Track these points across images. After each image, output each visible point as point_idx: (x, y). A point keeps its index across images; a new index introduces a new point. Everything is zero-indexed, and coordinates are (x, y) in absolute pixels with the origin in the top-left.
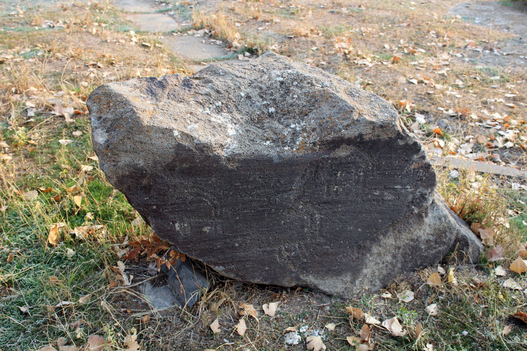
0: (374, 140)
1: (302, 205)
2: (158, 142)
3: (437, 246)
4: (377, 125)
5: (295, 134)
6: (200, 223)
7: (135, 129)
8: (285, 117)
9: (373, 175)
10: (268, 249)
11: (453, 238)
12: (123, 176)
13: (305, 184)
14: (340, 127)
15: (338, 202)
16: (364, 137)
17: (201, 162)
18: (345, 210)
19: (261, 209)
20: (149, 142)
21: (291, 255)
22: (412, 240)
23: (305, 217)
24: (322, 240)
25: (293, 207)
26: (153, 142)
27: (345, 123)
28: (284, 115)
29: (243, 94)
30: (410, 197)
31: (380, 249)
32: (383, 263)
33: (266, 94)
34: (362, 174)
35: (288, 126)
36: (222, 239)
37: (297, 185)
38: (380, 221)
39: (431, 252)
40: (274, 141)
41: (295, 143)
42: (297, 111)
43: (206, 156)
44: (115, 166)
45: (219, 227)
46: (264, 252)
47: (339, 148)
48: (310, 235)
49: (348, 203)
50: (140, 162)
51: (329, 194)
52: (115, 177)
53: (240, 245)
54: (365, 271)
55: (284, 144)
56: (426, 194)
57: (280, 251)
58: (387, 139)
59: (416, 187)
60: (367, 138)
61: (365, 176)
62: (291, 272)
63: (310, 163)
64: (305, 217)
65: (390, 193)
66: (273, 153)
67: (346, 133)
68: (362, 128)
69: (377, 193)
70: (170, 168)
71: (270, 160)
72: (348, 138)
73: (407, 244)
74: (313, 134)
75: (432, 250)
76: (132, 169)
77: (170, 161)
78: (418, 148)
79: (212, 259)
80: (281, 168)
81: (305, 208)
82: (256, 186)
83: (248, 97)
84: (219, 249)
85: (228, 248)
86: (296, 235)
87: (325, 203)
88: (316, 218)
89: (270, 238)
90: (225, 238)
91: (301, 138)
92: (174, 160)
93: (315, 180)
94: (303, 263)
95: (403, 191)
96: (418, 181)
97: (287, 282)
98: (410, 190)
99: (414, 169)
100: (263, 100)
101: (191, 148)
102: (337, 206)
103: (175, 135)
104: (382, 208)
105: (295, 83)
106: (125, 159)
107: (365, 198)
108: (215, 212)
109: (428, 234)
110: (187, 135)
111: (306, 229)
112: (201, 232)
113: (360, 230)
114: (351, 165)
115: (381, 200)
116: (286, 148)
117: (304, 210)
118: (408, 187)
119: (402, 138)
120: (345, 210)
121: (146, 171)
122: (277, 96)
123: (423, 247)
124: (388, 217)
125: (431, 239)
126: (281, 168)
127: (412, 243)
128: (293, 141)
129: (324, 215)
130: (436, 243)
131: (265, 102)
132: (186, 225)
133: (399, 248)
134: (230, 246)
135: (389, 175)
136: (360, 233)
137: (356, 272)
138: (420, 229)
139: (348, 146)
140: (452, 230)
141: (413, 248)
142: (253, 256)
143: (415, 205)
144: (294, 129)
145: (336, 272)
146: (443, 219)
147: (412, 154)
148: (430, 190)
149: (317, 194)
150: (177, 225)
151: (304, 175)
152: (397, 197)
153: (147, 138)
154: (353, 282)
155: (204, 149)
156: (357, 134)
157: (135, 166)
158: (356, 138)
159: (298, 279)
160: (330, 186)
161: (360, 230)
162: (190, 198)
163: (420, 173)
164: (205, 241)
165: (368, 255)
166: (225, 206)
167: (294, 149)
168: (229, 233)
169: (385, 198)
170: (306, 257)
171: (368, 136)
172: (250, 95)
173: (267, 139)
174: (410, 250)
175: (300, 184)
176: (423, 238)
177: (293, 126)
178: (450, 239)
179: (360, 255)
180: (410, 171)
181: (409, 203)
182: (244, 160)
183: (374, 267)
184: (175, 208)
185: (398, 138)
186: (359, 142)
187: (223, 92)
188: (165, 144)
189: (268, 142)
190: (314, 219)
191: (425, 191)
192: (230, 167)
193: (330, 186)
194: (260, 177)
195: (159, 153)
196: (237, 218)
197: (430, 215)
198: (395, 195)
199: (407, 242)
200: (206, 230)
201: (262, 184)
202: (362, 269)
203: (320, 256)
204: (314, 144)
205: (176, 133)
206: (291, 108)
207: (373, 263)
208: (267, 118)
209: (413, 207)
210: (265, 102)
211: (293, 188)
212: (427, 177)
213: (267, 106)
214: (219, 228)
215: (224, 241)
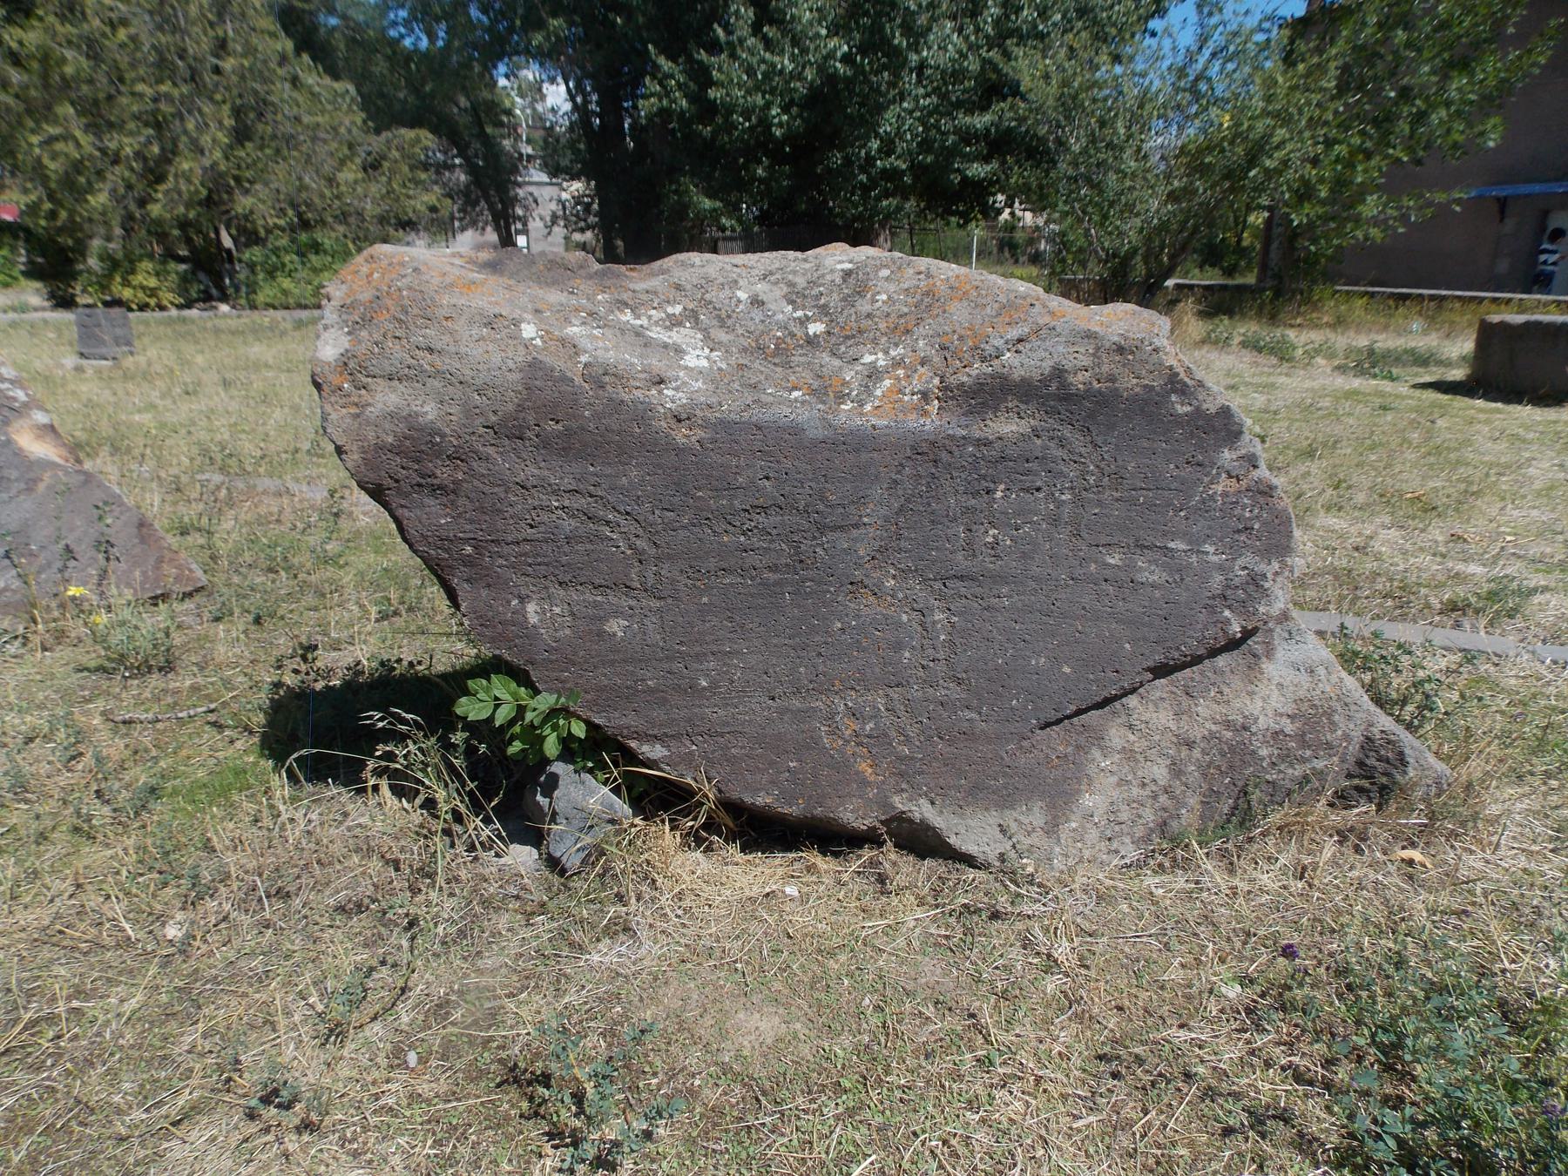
0: (1099, 391)
1: (894, 577)
2: (477, 351)
3: (1308, 753)
4: (1107, 345)
5: (874, 374)
6: (596, 605)
7: (416, 311)
8: (849, 343)
9: (1100, 503)
10: (796, 703)
11: (1357, 736)
12: (380, 447)
14: (999, 343)
16: (1071, 379)
17: (597, 416)
18: (1020, 605)
19: (772, 576)
20: (452, 349)
21: (863, 729)
22: (1228, 724)
23: (905, 618)
24: (955, 692)
25: (866, 581)
26: (463, 350)
27: (1014, 333)
28: (847, 338)
29: (742, 295)
30: (1217, 580)
31: (1132, 738)
32: (1144, 785)
33: (805, 297)
36: (660, 660)
39: (1290, 771)
40: (813, 392)
42: (882, 326)
43: (610, 399)
44: (358, 416)
45: (651, 623)
46: (782, 712)
47: (996, 409)
48: (921, 673)
49: (1030, 582)
50: (427, 408)
51: (970, 549)
52: (355, 448)
53: (714, 685)
54: (1088, 801)
55: (841, 398)
56: (1264, 576)
57: (831, 716)
58: (1137, 390)
59: (1235, 551)
60: (1078, 381)
61: (1078, 501)
62: (864, 783)
63: (913, 448)
64: (905, 618)
65: (1155, 562)
66: (803, 416)
67: (1016, 363)
68: (1061, 349)
69: (1114, 560)
70: (510, 431)
71: (796, 430)
72: (1023, 380)
74: (922, 370)
75: (1291, 765)
76: (402, 428)
77: (511, 407)
79: (631, 720)
80: (826, 454)
82: (756, 503)
83: (757, 302)
84: (652, 691)
85: (677, 688)
87: (962, 578)
88: (934, 623)
90: (669, 659)
91: (887, 383)
92: (521, 408)
94: (901, 759)
95: (1194, 558)
96: (1239, 531)
97: (852, 811)
98: (1215, 559)
99: (1225, 494)
100: (795, 310)
101: (569, 374)
102: (995, 592)
104: (1131, 606)
106: (386, 399)
107: (1078, 572)
108: (641, 575)
109: (1278, 714)
110: (563, 342)
111: (907, 654)
112: (600, 634)
113: (1067, 670)
115: (1128, 584)
117: (901, 595)
118: (1210, 548)
119: (1183, 391)
120: (1020, 605)
121: (443, 436)
122: (834, 300)
123: (1264, 752)
124: (1153, 636)
125: (1288, 730)
126: (826, 454)
127: (1229, 734)
128: (868, 390)
129: (960, 614)
130: (1304, 744)
131: (799, 314)
132: (557, 610)
133: (1190, 745)
134: (684, 683)
135: (1151, 506)
137: (1059, 797)
138: (1251, 694)
139: (1023, 407)
140: (1353, 707)
141: (1232, 749)
142: (750, 721)
143: (1229, 607)
145: (991, 789)
147: (1218, 448)
148: (1276, 566)
150: (531, 608)
152: (1177, 577)
153: (447, 338)
154: (1052, 829)
155: (607, 379)
156: (1047, 366)
157: (410, 418)
158: (1045, 381)
159: (886, 805)
160: (974, 527)
161: (1067, 670)
162: (569, 524)
163: (1243, 509)
164: (612, 663)
165: (1096, 753)
166: (669, 557)
167: (868, 407)
168: (681, 643)
169: (1142, 577)
170: (908, 740)
173: (795, 388)
174: (1223, 755)
175: (884, 511)
177: (868, 359)
178: (1346, 737)
179: (1070, 749)
180: (1212, 498)
181: (1214, 597)
182: (721, 421)
183: (1115, 794)
184: (525, 554)
185: (1174, 391)
186: (1052, 395)
187: (689, 287)
188: (496, 359)
189: (796, 394)
191: (1262, 567)
192: (680, 440)
193: (974, 527)
194: (767, 478)
195: (478, 382)
196: (705, 600)
197: (1280, 654)
199: (1214, 728)
200: (616, 628)
201: (774, 498)
202: (1078, 792)
203: (951, 742)
204: (925, 396)
205: (528, 331)
206: (866, 323)
207: (1114, 779)
208: (802, 346)
209: (1227, 613)
210: (799, 314)
212: (1264, 524)
213: (804, 322)
214: (651, 626)
215: (666, 666)
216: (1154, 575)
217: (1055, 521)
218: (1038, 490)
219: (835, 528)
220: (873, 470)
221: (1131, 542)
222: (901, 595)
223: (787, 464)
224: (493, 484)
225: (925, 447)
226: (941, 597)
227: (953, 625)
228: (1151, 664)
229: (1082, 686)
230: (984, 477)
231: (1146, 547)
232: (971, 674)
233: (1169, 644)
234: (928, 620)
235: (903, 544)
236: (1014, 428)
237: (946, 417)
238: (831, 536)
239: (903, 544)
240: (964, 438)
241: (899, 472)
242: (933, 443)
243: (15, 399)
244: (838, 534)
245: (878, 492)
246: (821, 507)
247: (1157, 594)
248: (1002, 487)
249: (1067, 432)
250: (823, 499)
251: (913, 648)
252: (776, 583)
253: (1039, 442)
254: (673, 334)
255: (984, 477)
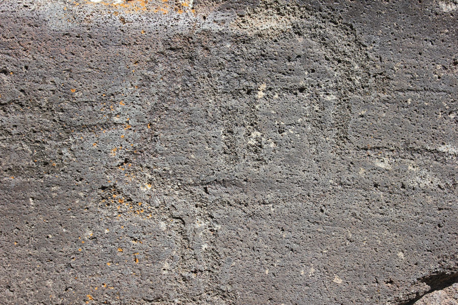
1: (150, 182)
13: (154, 110)
15: (265, 183)
19: (14, 180)
25: (119, 186)
34: (332, 98)
37: (127, 111)
38: (401, 255)
48: (183, 286)
51: (231, 151)
61: (344, 102)
63: (165, 42)
64: (163, 225)
71: (37, 22)
80: (71, 48)
81: (158, 194)
86: (134, 282)
87: (224, 183)
89: (50, 283)
93: (187, 105)
102: (260, 198)
111: (166, 266)
113: (338, 280)
114: (296, 64)
126: (71, 48)
129: (224, 222)
136: (340, 291)
149: (196, 151)
151: (147, 78)
152: (450, 182)
161: (338, 280)
175: (137, 110)
190: (190, 234)
198: (436, 171)
201: (13, 94)
211: (116, 119)
216: (429, 181)
217: (320, 123)
218: (302, 90)
219: (82, 128)
220: (123, 66)
221: (401, 144)
222: (157, 202)
223: (28, 58)
225: (178, 43)
226: (202, 203)
227: (215, 233)
228: (426, 273)
229: (354, 298)
230: (242, 76)
231: (417, 151)
232: (236, 286)
233: (443, 253)
234: (189, 228)
235: (158, 146)
236: (274, 24)
237: (202, 11)
238: (78, 136)
239: (158, 146)
240: (220, 33)
241: (151, 69)
242: (188, 38)
244: (86, 134)
245: (128, 89)
246: (66, 105)
247: (430, 200)
248: (263, 86)
249: (330, 30)
250: (68, 96)
251: (172, 258)
252: (17, 188)
253: (300, 40)
255: (242, 76)
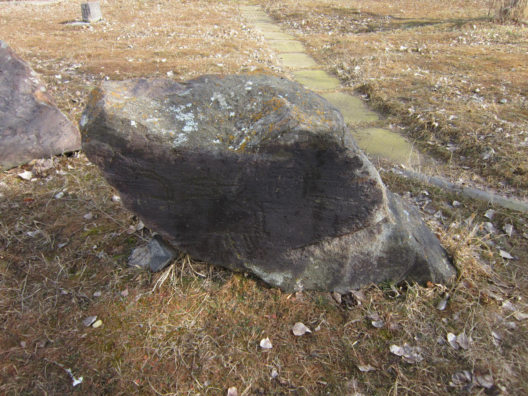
3: (392, 264)
22: (362, 253)
23: (249, 212)
35: (240, 129)
41: (238, 144)
55: (231, 143)
73: (355, 256)
78: (360, 163)
103: (132, 124)
105: (260, 93)
116: (231, 147)
127: (362, 256)
144: (243, 132)
146: (399, 239)
167: (236, 149)
171: (304, 144)
172: (219, 100)
174: (360, 263)
176: (375, 254)
189: (218, 141)
199: (356, 254)
205: (133, 123)
218: (293, 177)
224: (125, 166)
243: (35, 83)
254: (185, 116)
